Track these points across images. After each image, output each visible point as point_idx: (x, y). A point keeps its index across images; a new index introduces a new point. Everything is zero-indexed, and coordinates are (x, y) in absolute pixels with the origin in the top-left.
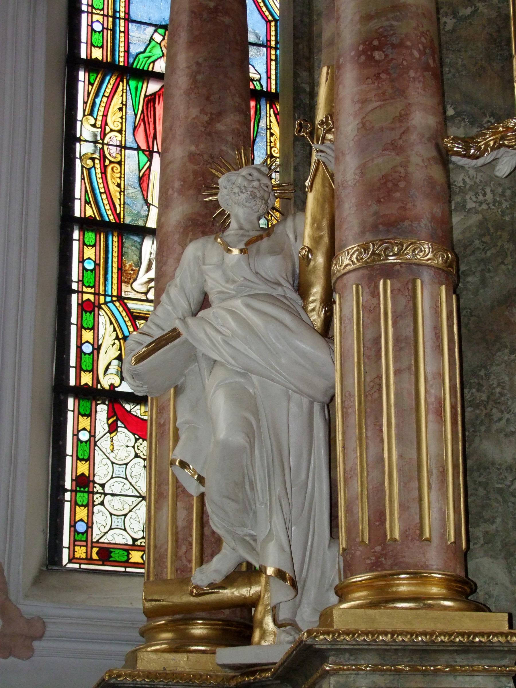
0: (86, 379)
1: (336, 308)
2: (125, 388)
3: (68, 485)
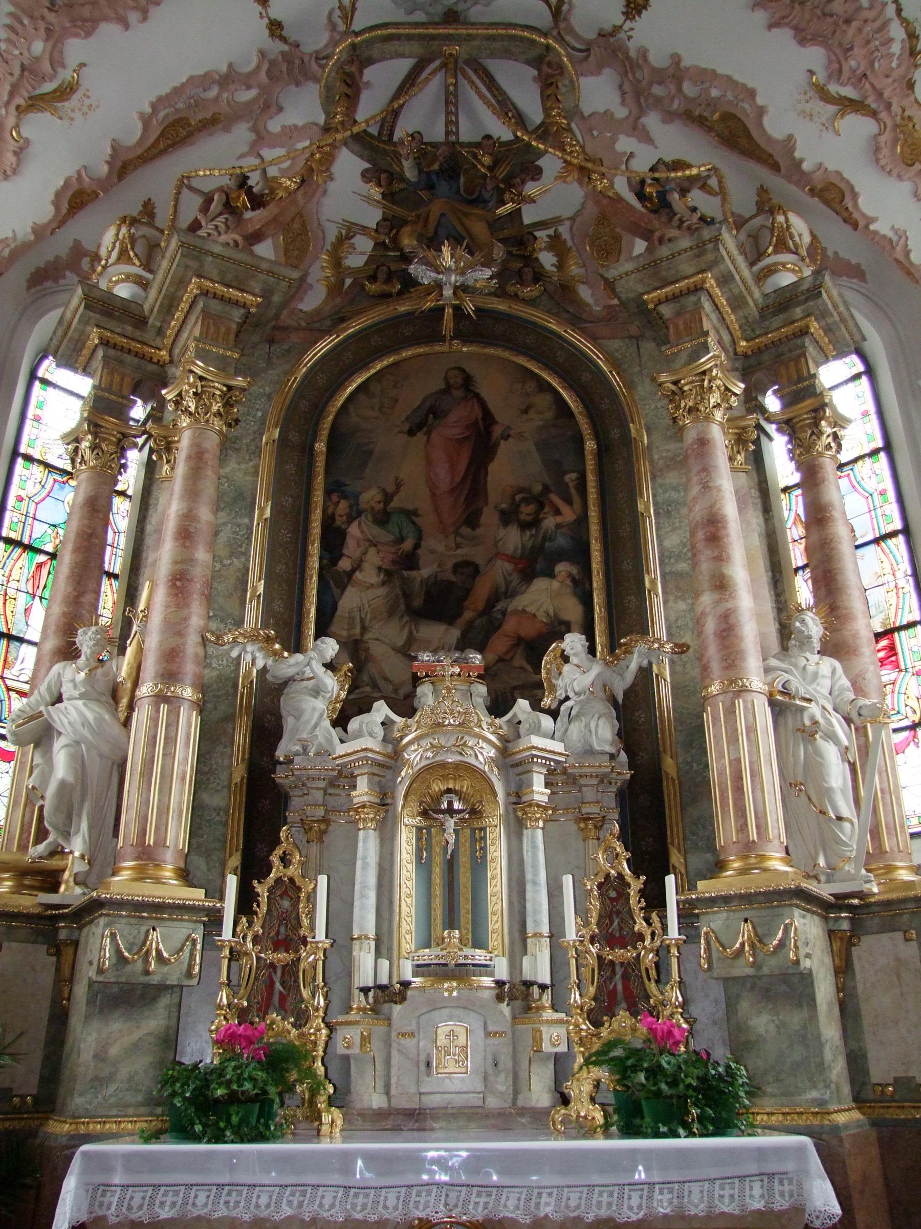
1: (135, 714)
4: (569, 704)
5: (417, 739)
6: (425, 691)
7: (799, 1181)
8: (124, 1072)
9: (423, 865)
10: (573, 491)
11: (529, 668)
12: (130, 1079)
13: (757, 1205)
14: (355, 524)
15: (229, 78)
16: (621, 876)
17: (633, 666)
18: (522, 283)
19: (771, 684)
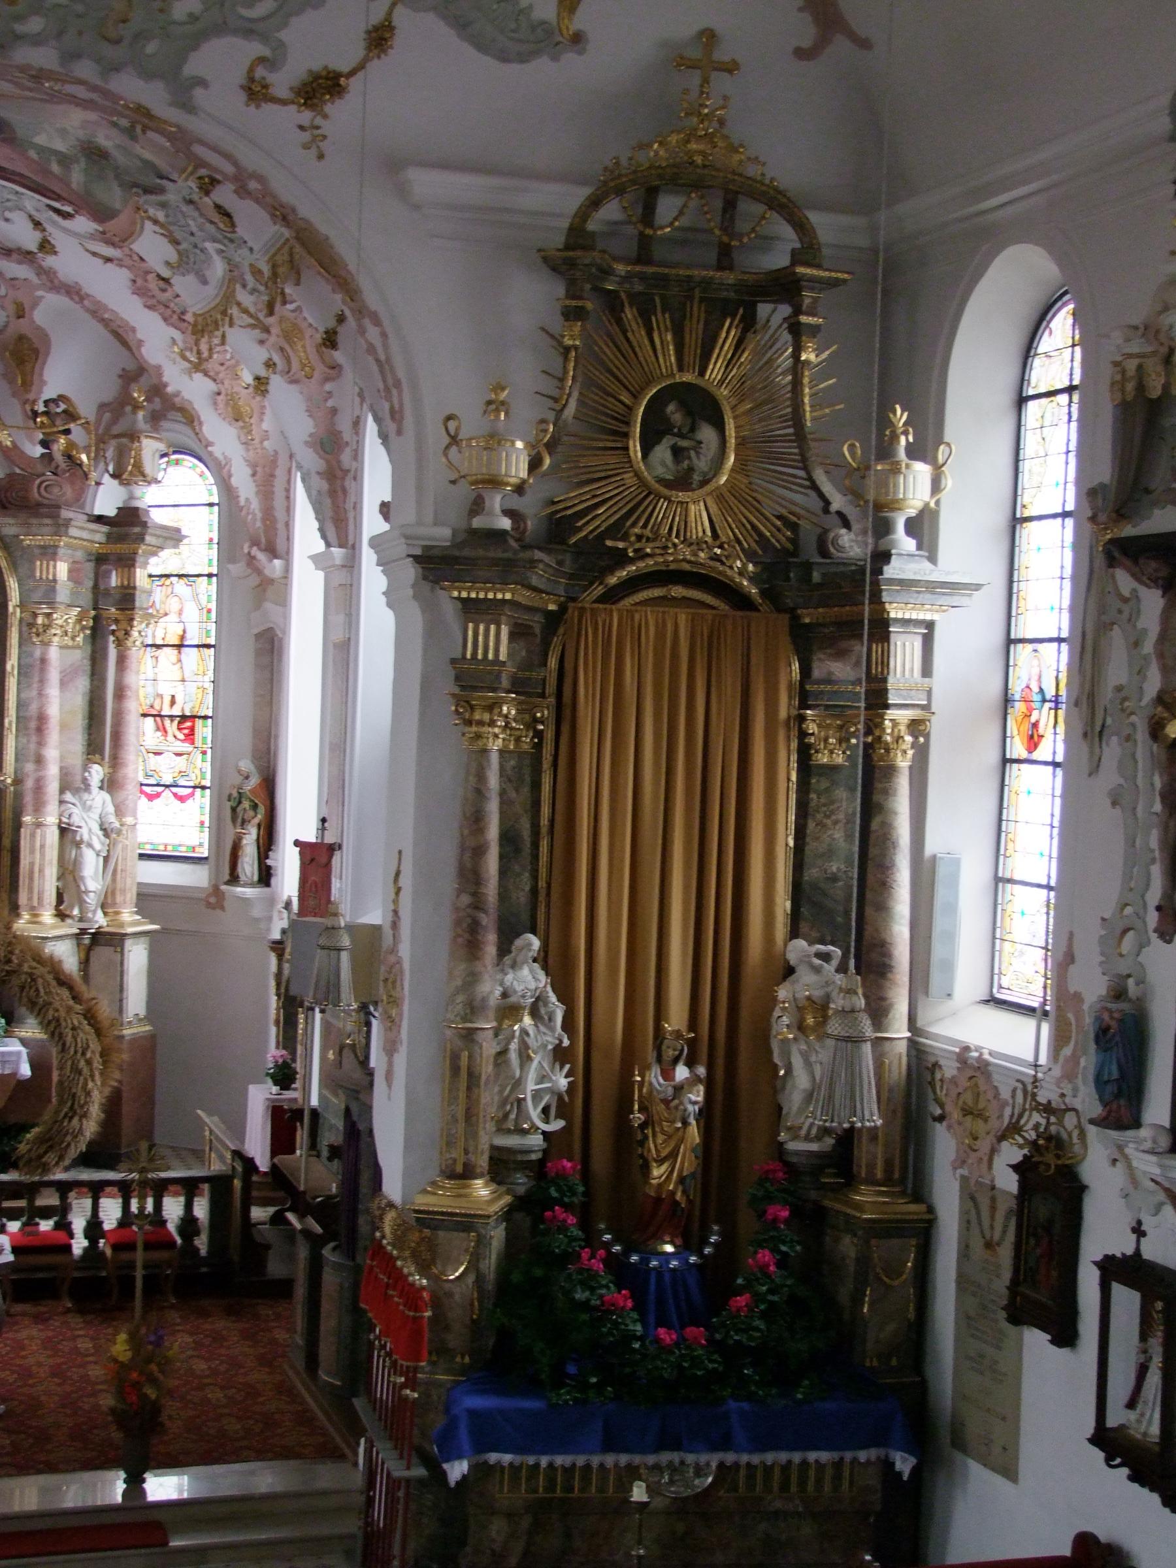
7: (17, 1063)
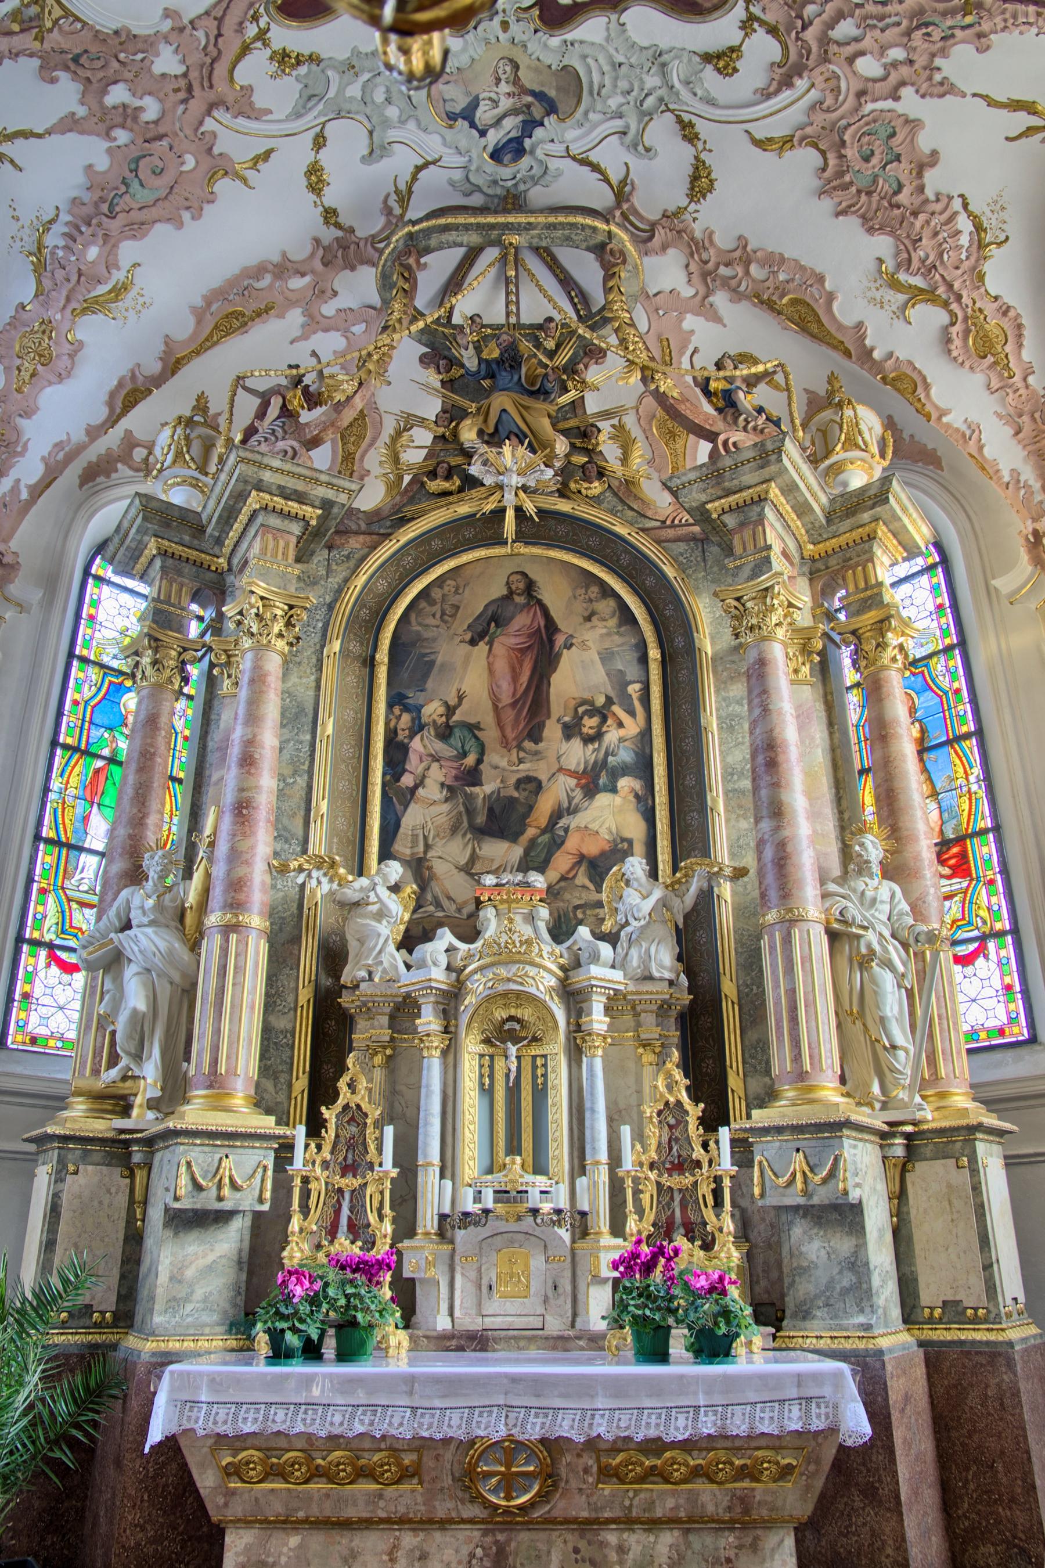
0: (36, 935)
1: (204, 942)
2: (58, 942)
3: (17, 997)
4: (629, 929)
5: (481, 969)
6: (489, 913)
8: (199, 1293)
9: (487, 1092)
10: (637, 704)
11: (592, 887)
12: (205, 1300)
13: (796, 1426)
14: (417, 738)
15: (283, 269)
16: (679, 1103)
17: (693, 889)
18: (587, 479)
19: (827, 911)
